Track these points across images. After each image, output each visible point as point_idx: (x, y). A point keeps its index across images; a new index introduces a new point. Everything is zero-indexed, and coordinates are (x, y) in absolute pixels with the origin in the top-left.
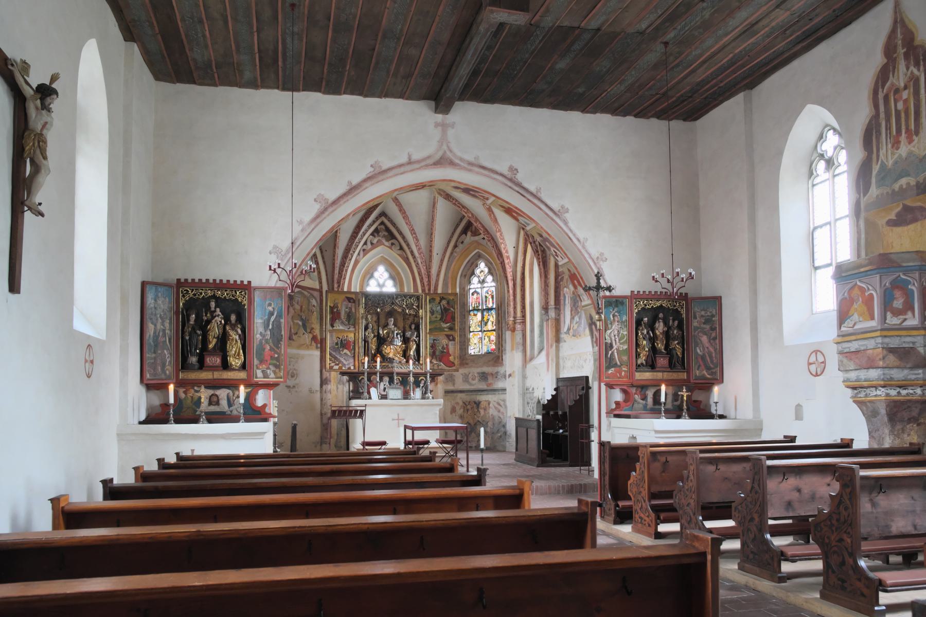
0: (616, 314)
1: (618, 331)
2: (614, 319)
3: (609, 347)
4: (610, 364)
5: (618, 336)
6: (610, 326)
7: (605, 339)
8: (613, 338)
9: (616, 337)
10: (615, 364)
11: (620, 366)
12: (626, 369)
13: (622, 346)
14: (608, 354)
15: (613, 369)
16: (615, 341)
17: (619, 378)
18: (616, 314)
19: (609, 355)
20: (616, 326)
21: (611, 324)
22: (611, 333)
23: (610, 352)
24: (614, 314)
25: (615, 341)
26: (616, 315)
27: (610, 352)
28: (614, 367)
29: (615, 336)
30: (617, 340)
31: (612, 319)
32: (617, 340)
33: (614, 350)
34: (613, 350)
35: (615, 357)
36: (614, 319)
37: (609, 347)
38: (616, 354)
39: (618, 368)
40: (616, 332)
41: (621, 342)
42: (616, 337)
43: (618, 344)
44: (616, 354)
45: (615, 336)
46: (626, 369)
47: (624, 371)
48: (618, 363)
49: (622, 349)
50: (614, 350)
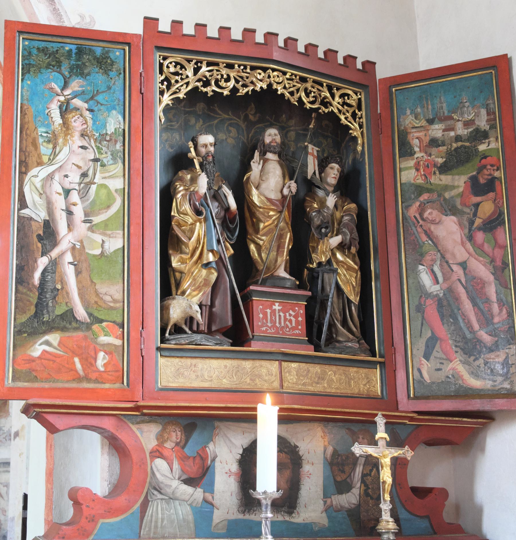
0: (77, 102)
1: (84, 175)
2: (66, 124)
3: (40, 238)
4: (37, 315)
5: (84, 194)
6: (45, 150)
7: (23, 204)
8: (60, 203)
9: (74, 197)
10: (62, 317)
11: (88, 327)
12: (118, 342)
13: (98, 238)
14: (34, 269)
15: (54, 338)
16: (69, 213)
17: (79, 379)
18: (77, 102)
19: (37, 275)
20: (71, 152)
21: (53, 140)
22: (50, 177)
23: (43, 262)
24: (68, 102)
25: (69, 213)
26: (77, 109)
27: (43, 262)
28: (63, 329)
29: (67, 192)
30: (79, 212)
31: (58, 120)
32: (79, 212)
33: (62, 254)
34: (54, 253)
35: (63, 282)
36: (66, 124)
37: (40, 238)
38: (70, 272)
39: (80, 334)
40: (75, 177)
41: (96, 220)
42: (74, 197)
43: (81, 228)
44: (70, 272)
45: (67, 192)
46: (118, 342)
47: (109, 349)
48: (81, 313)
49: (98, 252)
50: (62, 254)
